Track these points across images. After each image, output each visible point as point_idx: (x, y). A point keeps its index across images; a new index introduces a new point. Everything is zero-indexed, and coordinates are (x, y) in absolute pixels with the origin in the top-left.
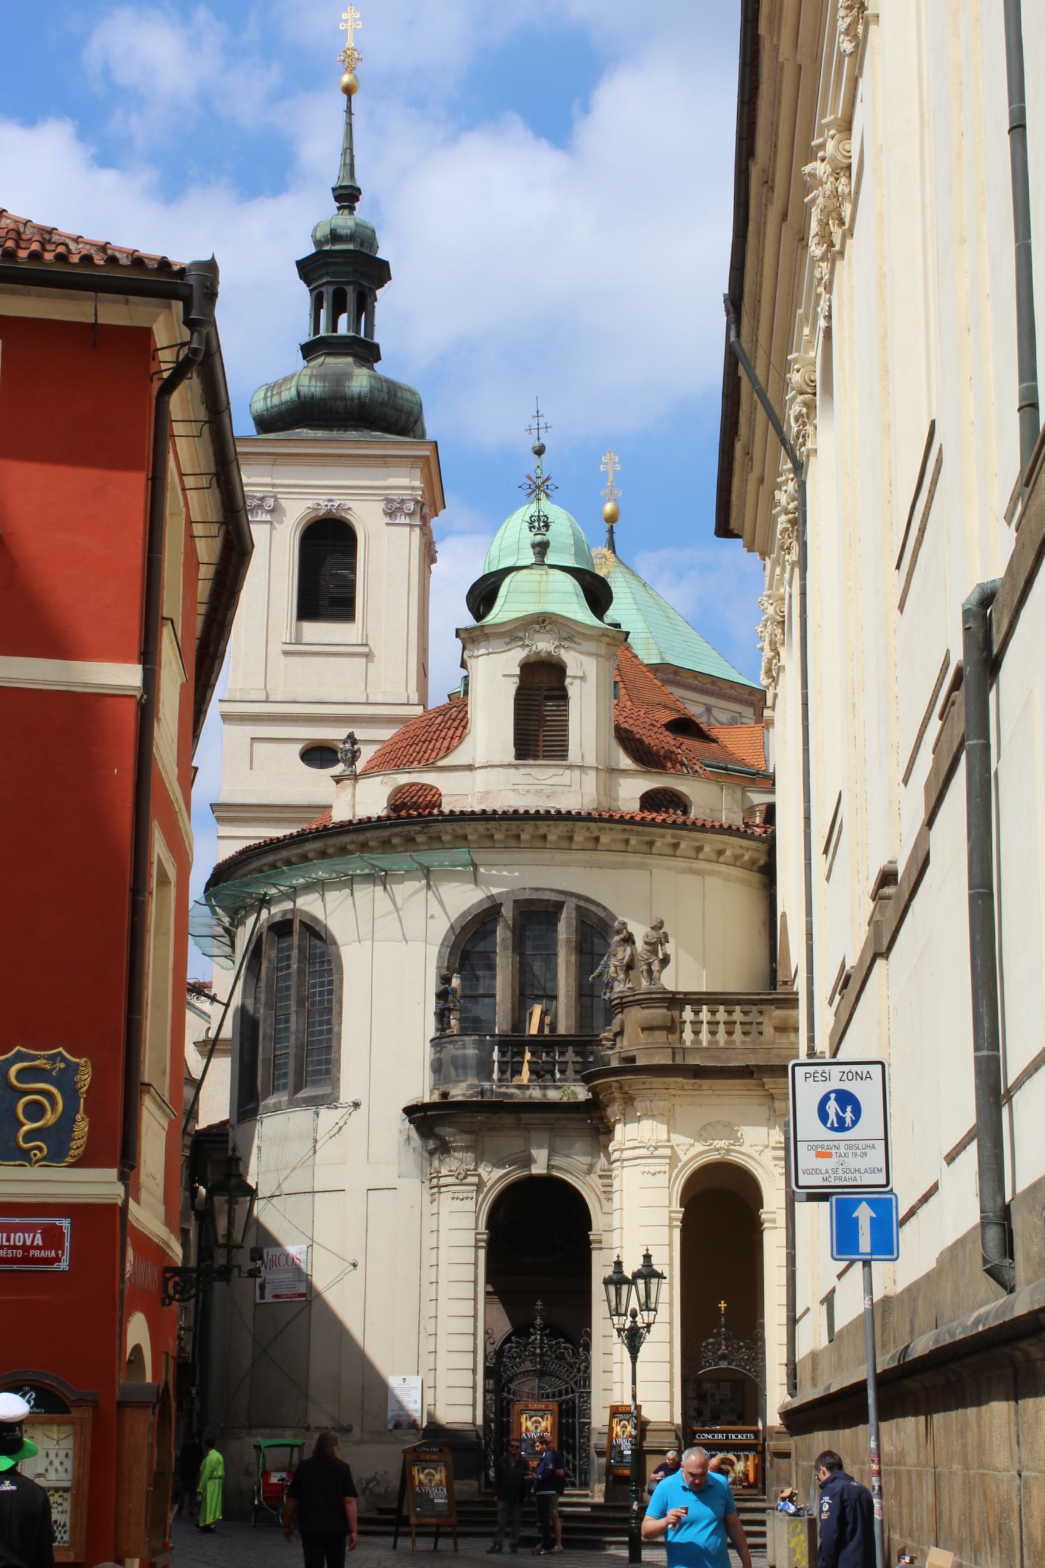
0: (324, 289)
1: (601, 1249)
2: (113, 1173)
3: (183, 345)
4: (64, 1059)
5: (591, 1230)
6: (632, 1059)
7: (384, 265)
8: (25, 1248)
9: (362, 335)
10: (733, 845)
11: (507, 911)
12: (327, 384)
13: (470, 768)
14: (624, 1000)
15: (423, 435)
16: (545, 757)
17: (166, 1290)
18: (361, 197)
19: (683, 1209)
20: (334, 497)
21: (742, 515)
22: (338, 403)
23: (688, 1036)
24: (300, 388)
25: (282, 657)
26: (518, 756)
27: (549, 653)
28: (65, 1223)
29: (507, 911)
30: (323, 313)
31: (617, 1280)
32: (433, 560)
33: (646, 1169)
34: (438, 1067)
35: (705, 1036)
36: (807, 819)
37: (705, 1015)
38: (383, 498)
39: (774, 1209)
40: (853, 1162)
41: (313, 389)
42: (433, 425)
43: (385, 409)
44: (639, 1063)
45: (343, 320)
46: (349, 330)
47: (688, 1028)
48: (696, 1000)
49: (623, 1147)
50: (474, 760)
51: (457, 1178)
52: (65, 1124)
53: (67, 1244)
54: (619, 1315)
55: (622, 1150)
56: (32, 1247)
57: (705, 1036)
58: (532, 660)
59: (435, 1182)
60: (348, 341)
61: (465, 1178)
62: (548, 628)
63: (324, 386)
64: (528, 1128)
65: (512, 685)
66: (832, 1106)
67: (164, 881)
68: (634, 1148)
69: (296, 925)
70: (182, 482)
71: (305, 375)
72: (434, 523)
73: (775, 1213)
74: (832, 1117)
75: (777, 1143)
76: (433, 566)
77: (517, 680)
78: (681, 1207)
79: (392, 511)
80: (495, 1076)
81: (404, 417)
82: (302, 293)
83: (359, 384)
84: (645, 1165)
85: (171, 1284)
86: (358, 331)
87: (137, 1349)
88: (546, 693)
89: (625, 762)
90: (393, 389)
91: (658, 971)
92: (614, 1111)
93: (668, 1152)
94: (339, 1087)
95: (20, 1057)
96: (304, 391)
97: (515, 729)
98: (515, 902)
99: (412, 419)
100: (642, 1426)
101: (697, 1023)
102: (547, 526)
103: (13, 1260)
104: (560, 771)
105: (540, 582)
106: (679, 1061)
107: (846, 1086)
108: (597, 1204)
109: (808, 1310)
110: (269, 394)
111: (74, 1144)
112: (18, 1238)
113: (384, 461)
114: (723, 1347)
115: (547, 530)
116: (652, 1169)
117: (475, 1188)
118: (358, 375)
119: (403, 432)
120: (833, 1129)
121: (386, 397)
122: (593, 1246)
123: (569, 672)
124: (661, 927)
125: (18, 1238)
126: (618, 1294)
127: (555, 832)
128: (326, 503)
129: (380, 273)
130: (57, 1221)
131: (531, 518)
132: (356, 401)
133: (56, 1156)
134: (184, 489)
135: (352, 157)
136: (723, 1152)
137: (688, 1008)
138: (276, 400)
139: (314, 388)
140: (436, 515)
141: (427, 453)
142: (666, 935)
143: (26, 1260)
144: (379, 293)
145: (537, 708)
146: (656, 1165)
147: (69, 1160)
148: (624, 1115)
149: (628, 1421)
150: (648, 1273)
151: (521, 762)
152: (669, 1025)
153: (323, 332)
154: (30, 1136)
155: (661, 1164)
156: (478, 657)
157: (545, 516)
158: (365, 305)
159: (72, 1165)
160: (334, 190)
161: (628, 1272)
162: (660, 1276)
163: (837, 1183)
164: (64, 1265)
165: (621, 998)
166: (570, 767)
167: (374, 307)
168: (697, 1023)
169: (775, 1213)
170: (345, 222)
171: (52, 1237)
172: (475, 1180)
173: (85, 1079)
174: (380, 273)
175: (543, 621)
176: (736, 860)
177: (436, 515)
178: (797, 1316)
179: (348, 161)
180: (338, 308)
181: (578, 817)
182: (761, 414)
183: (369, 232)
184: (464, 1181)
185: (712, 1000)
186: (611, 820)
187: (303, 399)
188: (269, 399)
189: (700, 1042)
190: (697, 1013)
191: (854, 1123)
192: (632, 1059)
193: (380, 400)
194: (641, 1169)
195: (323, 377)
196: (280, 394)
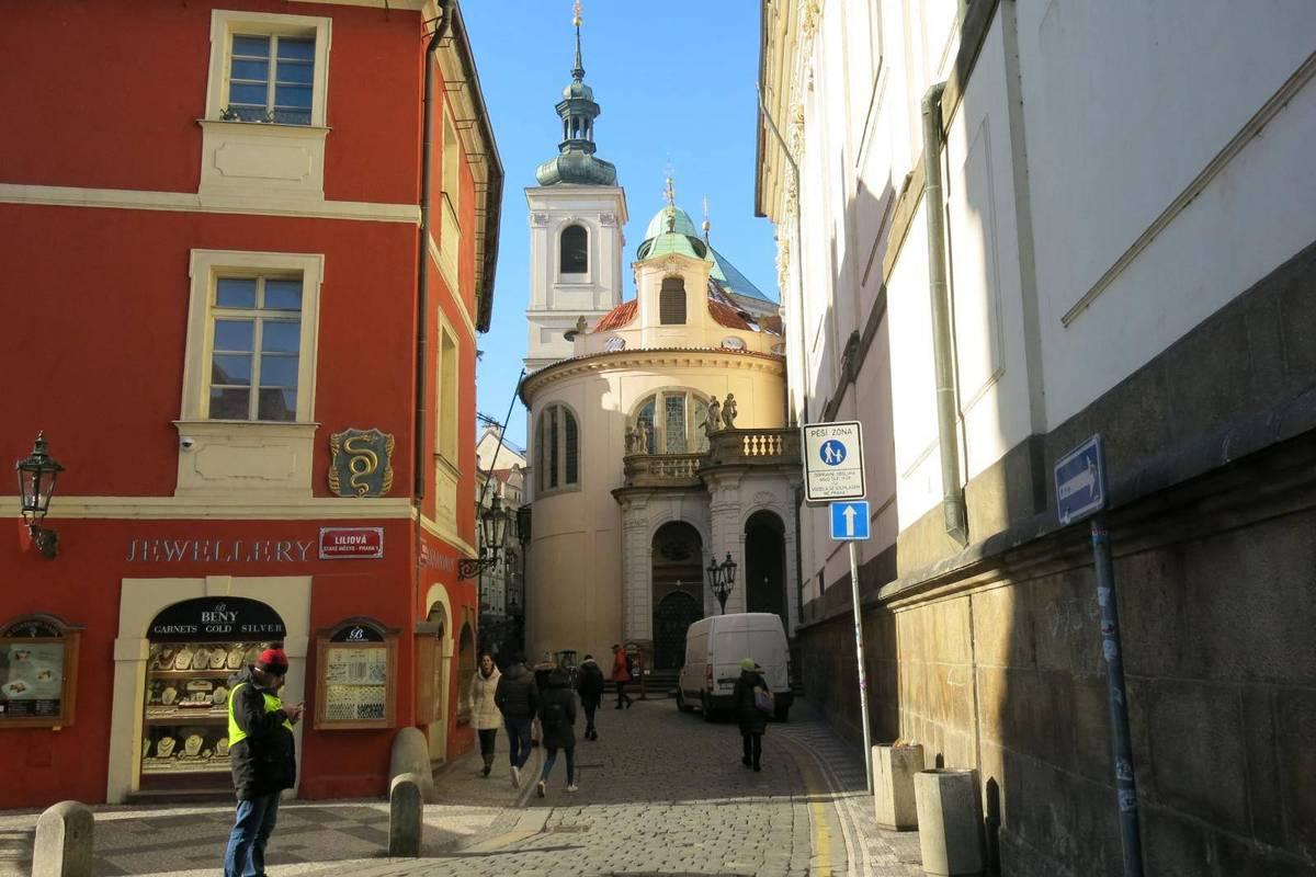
2: (408, 501)
3: (439, 18)
4: (377, 435)
6: (720, 462)
7: (597, 106)
8: (356, 545)
10: (766, 363)
11: (659, 397)
17: (460, 572)
21: (767, 209)
23: (747, 451)
26: (662, 323)
28: (380, 531)
31: (714, 569)
35: (755, 451)
36: (803, 341)
37: (755, 440)
40: (841, 482)
42: (621, 179)
44: (724, 464)
45: (578, 133)
47: (747, 446)
48: (751, 433)
52: (379, 474)
53: (382, 543)
54: (716, 585)
56: (361, 544)
57: (755, 451)
64: (669, 499)
66: (829, 450)
67: (448, 343)
70: (456, 126)
72: (624, 228)
74: (829, 456)
79: (603, 219)
82: (558, 123)
85: (463, 568)
87: (438, 606)
92: (711, 487)
95: (350, 434)
98: (663, 393)
101: (751, 445)
103: (350, 553)
106: (743, 462)
107: (837, 438)
109: (809, 580)
111: (384, 485)
112: (352, 540)
113: (599, 197)
119: (608, 184)
120: (829, 463)
125: (352, 540)
126: (715, 576)
129: (594, 110)
130: (375, 530)
133: (375, 491)
134: (457, 129)
143: (357, 552)
147: (382, 493)
150: (729, 565)
153: (569, 138)
154: (359, 480)
158: (588, 124)
159: (385, 496)
161: (719, 564)
162: (735, 565)
163: (833, 495)
164: (380, 554)
168: (751, 445)
170: (578, 87)
171: (373, 540)
173: (391, 447)
174: (594, 110)
175: (672, 258)
182: (776, 141)
185: (759, 432)
190: (751, 439)
191: (842, 459)
192: (720, 462)
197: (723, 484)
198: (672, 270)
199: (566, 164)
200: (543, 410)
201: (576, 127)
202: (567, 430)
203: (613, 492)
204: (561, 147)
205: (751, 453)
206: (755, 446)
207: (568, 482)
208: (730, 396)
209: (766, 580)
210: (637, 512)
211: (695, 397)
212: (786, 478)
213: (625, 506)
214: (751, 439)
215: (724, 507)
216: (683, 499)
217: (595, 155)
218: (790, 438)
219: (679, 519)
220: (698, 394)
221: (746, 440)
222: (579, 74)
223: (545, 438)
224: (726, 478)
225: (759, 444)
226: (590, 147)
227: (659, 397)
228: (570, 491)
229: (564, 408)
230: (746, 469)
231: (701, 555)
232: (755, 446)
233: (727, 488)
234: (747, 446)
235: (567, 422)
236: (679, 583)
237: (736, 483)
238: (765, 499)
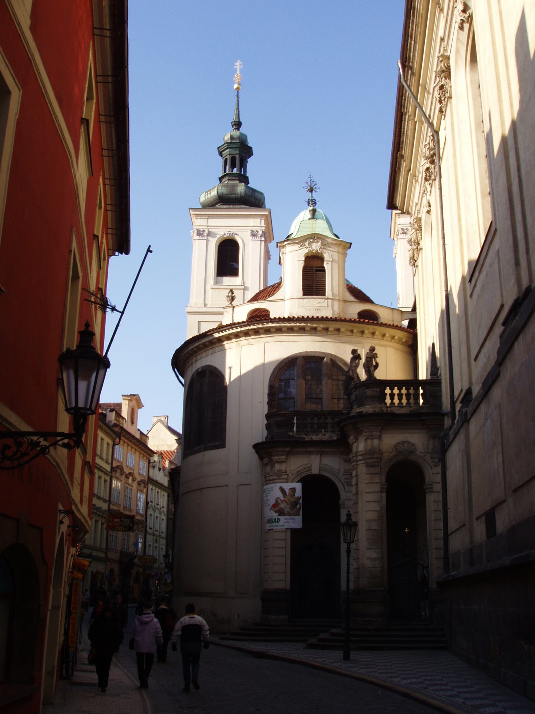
0: (228, 157)
1: (345, 508)
5: (340, 499)
9: (242, 173)
10: (399, 334)
13: (283, 300)
15: (265, 207)
16: (316, 295)
18: (242, 126)
19: (387, 484)
20: (230, 230)
22: (232, 195)
23: (388, 401)
25: (211, 290)
26: (304, 295)
30: (227, 167)
32: (269, 259)
34: (268, 427)
35: (396, 401)
37: (396, 391)
41: (223, 191)
42: (268, 203)
43: (250, 199)
46: (237, 171)
47: (388, 397)
48: (392, 384)
50: (285, 297)
51: (277, 476)
57: (396, 401)
58: (310, 255)
59: (268, 478)
60: (237, 175)
61: (281, 476)
63: (227, 190)
64: (310, 453)
69: (208, 372)
71: (220, 186)
76: (269, 261)
79: (254, 234)
80: (295, 429)
83: (240, 189)
86: (241, 171)
88: (316, 269)
89: (352, 298)
90: (254, 191)
94: (225, 440)
96: (220, 191)
97: (303, 284)
99: (261, 203)
101: (392, 396)
102: (315, 203)
104: (323, 300)
105: (313, 224)
108: (342, 487)
110: (206, 194)
115: (315, 205)
121: (251, 194)
122: (341, 506)
128: (228, 233)
131: (308, 200)
132: (239, 195)
135: (239, 112)
137: (388, 388)
138: (209, 196)
140: (271, 242)
141: (267, 213)
142: (376, 354)
144: (249, 160)
145: (312, 275)
151: (306, 297)
153: (227, 172)
157: (315, 199)
158: (243, 164)
160: (232, 123)
166: (327, 299)
167: (247, 165)
168: (392, 396)
170: (236, 134)
172: (286, 477)
175: (314, 237)
177: (271, 242)
178: (449, 532)
179: (237, 113)
180: (233, 166)
181: (331, 320)
183: (245, 137)
184: (281, 477)
186: (345, 320)
187: (219, 194)
188: (206, 196)
190: (392, 389)
195: (226, 186)
196: (210, 193)
198: (316, 247)
199: (224, 191)
200: (193, 375)
201: (233, 166)
204: (221, 179)
205: (392, 403)
206: (396, 397)
208: (372, 349)
209: (407, 530)
214: (392, 389)
216: (322, 454)
217: (249, 185)
221: (388, 391)
222: (238, 125)
225: (400, 395)
226: (244, 179)
227: (298, 362)
232: (396, 397)
234: (388, 397)
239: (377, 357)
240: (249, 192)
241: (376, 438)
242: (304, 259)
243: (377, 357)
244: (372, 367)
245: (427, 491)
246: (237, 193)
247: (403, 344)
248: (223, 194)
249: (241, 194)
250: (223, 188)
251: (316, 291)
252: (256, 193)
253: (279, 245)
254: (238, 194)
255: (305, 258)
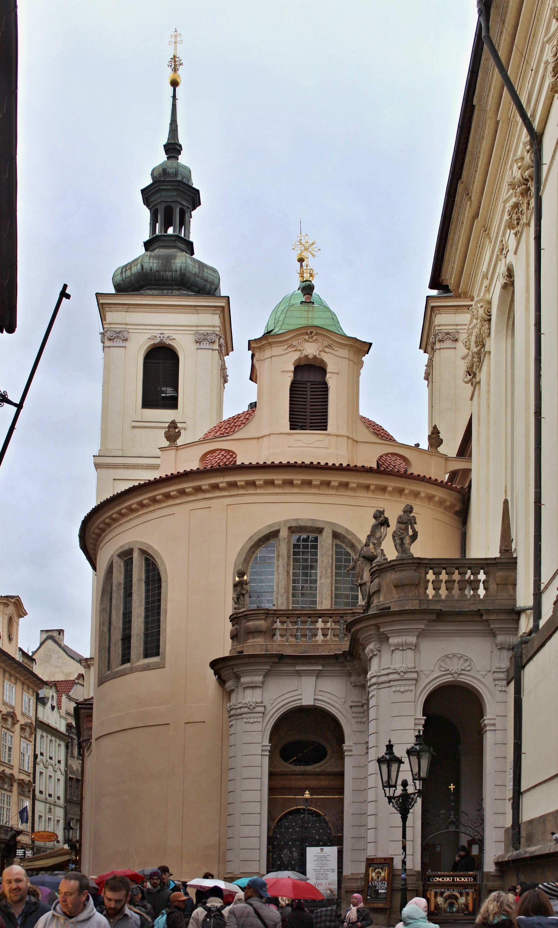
10: (439, 493)
11: (284, 533)
12: (160, 261)
14: (381, 567)
19: (425, 718)
22: (167, 273)
23: (430, 592)
24: (144, 264)
26: (293, 427)
27: (315, 357)
29: (284, 533)
33: (398, 689)
37: (444, 576)
38: (193, 332)
39: (495, 717)
43: (197, 279)
47: (430, 585)
49: (379, 674)
55: (379, 676)
57: (443, 592)
58: (302, 364)
62: (314, 338)
63: (159, 263)
65: (288, 379)
68: (388, 674)
73: (495, 719)
75: (497, 668)
77: (292, 375)
78: (423, 716)
81: (208, 286)
83: (180, 261)
84: (396, 686)
90: (202, 266)
91: (408, 544)
93: (415, 676)
96: (146, 266)
100: (392, 874)
106: (424, 607)
114: (452, 817)
116: (402, 689)
117: (261, 715)
118: (180, 256)
121: (197, 271)
123: (328, 370)
124: (411, 512)
127: (317, 478)
132: (178, 272)
136: (455, 675)
139: (152, 264)
146: (405, 685)
148: (380, 651)
149: (382, 869)
152: (417, 583)
155: (409, 685)
156: (264, 360)
165: (379, 565)
169: (495, 719)
176: (441, 503)
189: (440, 596)
192: (389, 608)
193: (193, 272)
194: (394, 689)
195: (158, 257)
197: (392, 641)
202: (147, 583)
203: (214, 664)
205: (437, 595)
207: (146, 655)
208: (409, 510)
210: (248, 692)
211: (336, 535)
212: (494, 634)
213: (230, 684)
214: (437, 574)
215: (391, 677)
217: (193, 256)
218: (500, 574)
219: (311, 703)
220: (339, 530)
221: (431, 576)
223: (114, 595)
224: (399, 633)
228: (147, 668)
229: (143, 552)
230: (434, 617)
231: (342, 758)
233: (399, 647)
234: (430, 585)
235: (147, 571)
236: (307, 795)
237: (412, 639)
238: (455, 666)
239: (416, 523)
240: (195, 267)
241: (411, 649)
242: (293, 370)
243: (416, 523)
244: (407, 537)
245: (488, 728)
246: (174, 269)
247: (448, 509)
248: (151, 270)
249: (181, 271)
250: (152, 260)
251: (311, 419)
252: (206, 270)
253: (253, 345)
254: (176, 271)
255: (295, 368)
